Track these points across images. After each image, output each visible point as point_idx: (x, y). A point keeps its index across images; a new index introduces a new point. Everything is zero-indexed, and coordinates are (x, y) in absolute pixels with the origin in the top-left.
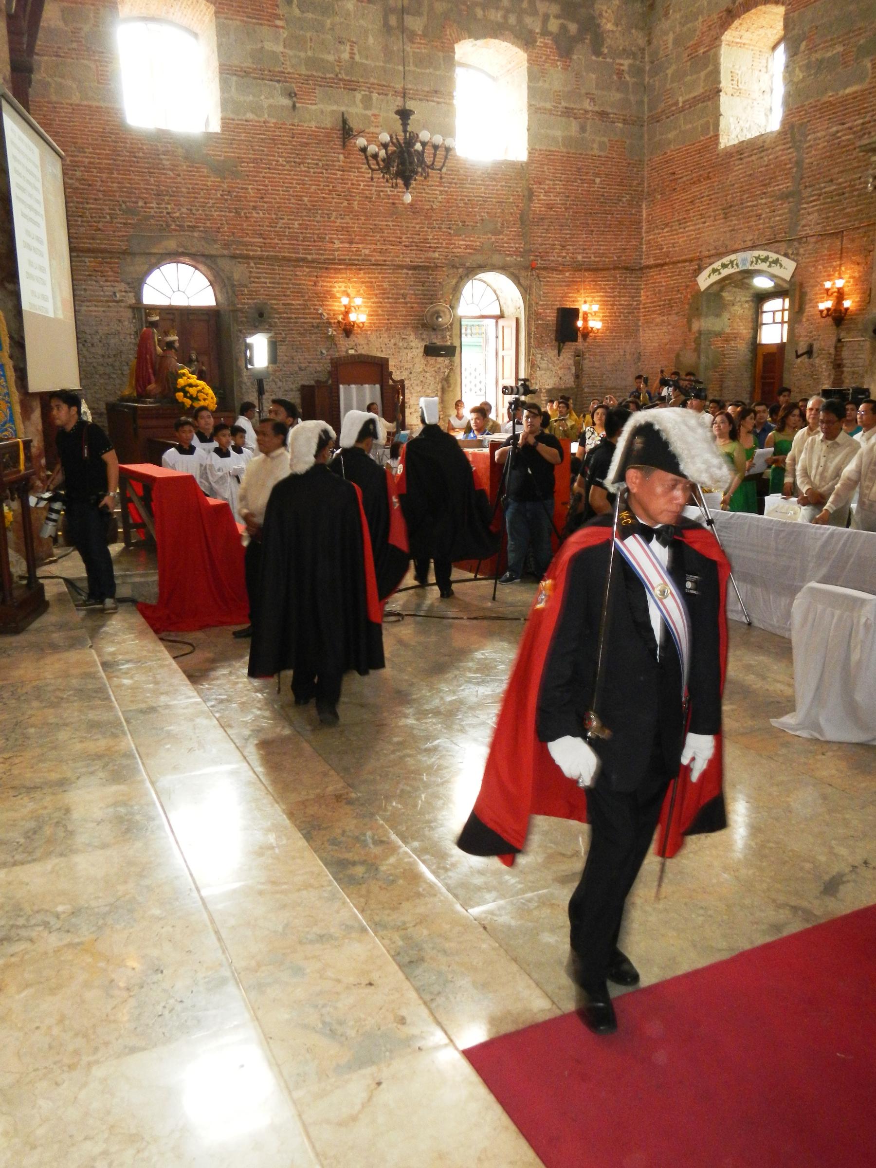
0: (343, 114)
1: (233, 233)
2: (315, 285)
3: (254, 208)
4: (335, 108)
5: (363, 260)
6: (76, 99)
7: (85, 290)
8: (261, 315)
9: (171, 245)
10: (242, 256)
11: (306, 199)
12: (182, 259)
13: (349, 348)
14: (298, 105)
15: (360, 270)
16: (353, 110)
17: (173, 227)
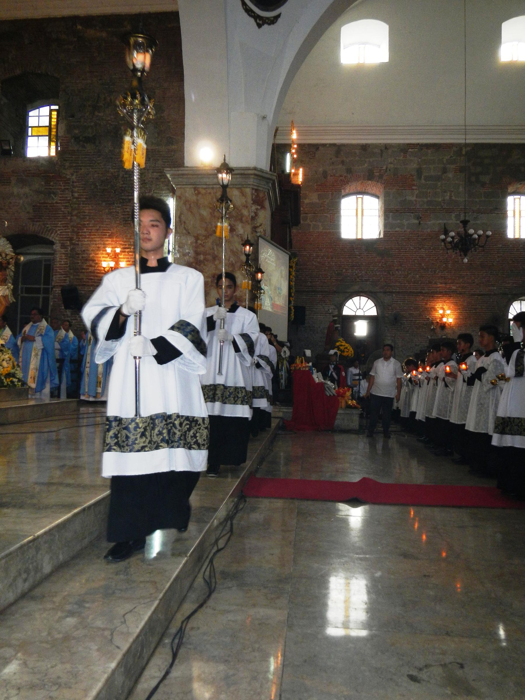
0: (445, 224)
1: (386, 282)
2: (426, 304)
3: (397, 270)
4: (441, 221)
5: (452, 292)
6: (321, 229)
7: (316, 309)
8: (396, 319)
9: (356, 288)
10: (390, 292)
11: (423, 264)
12: (361, 294)
13: (440, 334)
14: (421, 222)
15: (451, 297)
16: (450, 222)
17: (358, 280)
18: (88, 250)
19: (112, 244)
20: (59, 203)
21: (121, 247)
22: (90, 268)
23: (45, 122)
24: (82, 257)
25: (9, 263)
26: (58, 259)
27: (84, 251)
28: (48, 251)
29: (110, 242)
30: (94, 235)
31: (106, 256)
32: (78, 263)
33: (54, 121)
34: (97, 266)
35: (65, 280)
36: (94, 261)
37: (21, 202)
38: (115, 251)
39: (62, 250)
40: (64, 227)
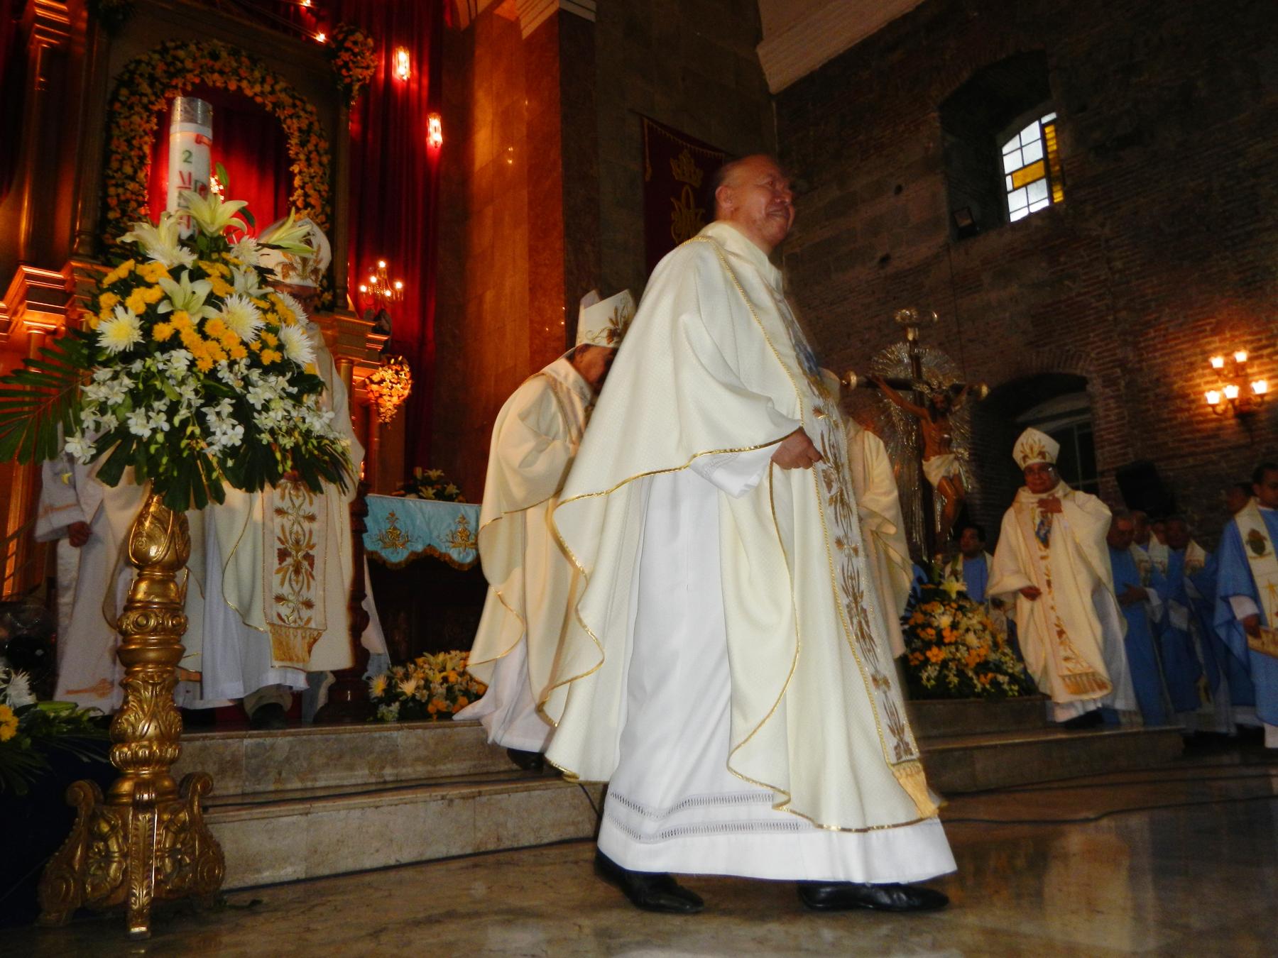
18: (1166, 376)
19: (1223, 348)
20: (1085, 293)
21: (1250, 347)
22: (1179, 415)
23: (1035, 152)
24: (1157, 395)
25: (948, 401)
26: (1101, 413)
27: (1158, 380)
28: (1081, 404)
29: (1217, 345)
30: (1175, 339)
31: (1215, 378)
32: (1149, 410)
33: (1053, 146)
34: (1194, 406)
35: (1125, 454)
36: (1184, 396)
37: (1007, 315)
38: (1234, 362)
39: (1107, 390)
40: (1101, 340)
